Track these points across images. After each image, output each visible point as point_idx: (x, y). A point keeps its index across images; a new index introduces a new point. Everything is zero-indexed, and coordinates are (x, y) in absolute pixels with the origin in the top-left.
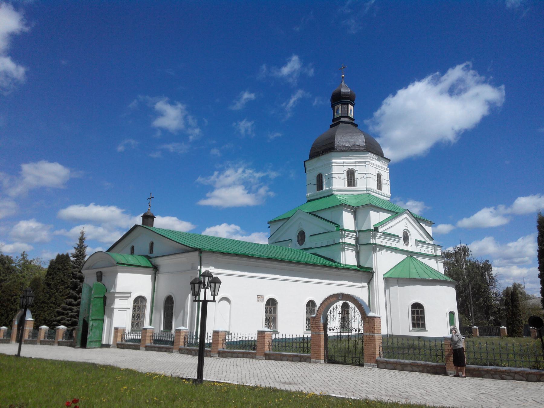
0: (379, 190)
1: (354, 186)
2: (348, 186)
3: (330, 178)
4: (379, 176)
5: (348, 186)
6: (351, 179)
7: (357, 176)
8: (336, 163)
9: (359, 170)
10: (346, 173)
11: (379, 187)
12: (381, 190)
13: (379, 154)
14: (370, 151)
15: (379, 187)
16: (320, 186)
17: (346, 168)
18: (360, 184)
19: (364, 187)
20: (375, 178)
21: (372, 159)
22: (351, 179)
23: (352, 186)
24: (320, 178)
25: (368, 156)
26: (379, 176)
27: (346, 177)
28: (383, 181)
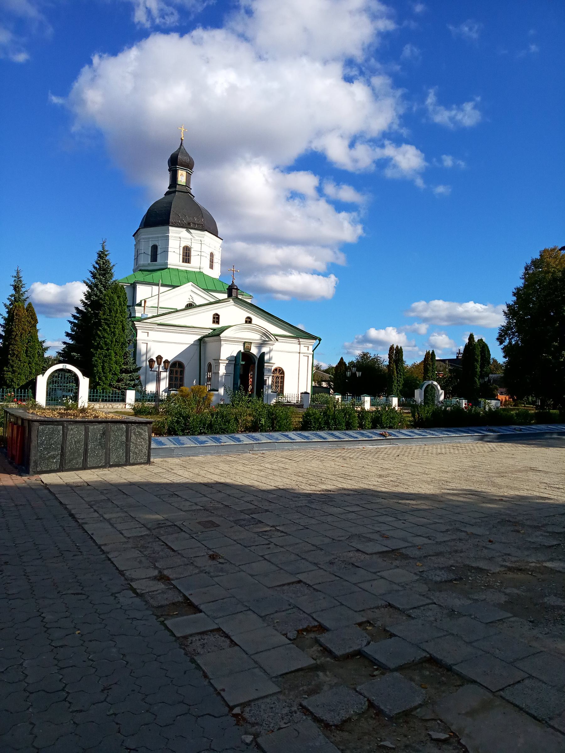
2: (183, 262)
3: (166, 251)
4: (212, 255)
5: (183, 262)
6: (187, 256)
7: (193, 253)
11: (211, 267)
12: (212, 269)
13: (215, 232)
14: (206, 230)
15: (211, 267)
16: (154, 258)
17: (183, 245)
20: (209, 257)
22: (187, 256)
23: (186, 262)
24: (155, 249)
25: (204, 235)
26: (212, 255)
27: (181, 253)
28: (215, 260)
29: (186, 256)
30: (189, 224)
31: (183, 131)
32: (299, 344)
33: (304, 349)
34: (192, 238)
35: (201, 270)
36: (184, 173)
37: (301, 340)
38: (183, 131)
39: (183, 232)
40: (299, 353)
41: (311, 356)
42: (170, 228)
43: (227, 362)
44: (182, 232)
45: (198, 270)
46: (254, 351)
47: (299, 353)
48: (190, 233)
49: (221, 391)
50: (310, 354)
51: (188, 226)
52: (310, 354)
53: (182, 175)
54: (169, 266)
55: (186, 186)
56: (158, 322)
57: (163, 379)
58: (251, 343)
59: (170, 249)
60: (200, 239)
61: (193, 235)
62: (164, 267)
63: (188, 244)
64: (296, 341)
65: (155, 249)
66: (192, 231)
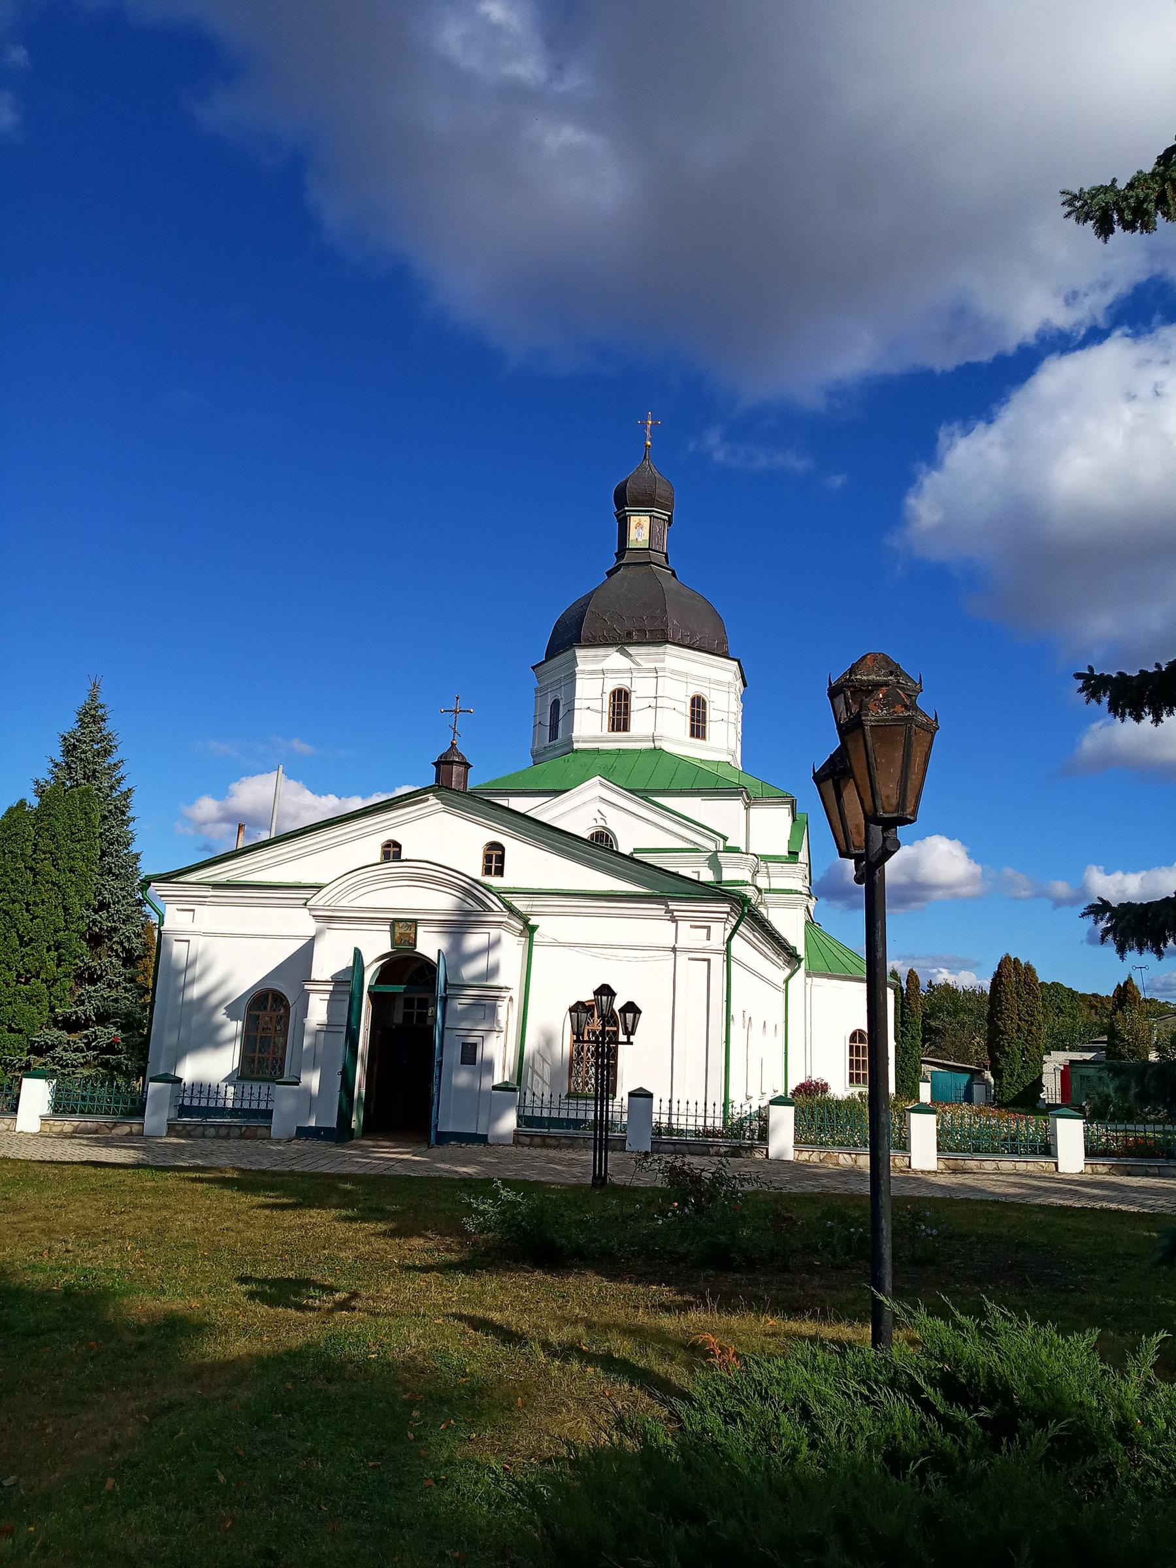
0: (698, 737)
1: (626, 729)
3: (571, 711)
4: (698, 706)
7: (635, 704)
8: (583, 672)
9: (641, 691)
10: (607, 698)
12: (704, 738)
14: (668, 642)
17: (611, 685)
18: (640, 722)
19: (648, 731)
21: (675, 658)
23: (619, 730)
24: (556, 704)
25: (664, 653)
26: (698, 706)
28: (711, 714)
29: (619, 714)
30: (629, 634)
31: (649, 426)
32: (674, 920)
33: (690, 936)
34: (633, 666)
35: (658, 744)
36: (645, 520)
37: (673, 906)
38: (649, 426)
39: (614, 659)
40: (674, 950)
41: (718, 961)
42: (580, 653)
43: (331, 988)
44: (608, 656)
45: (650, 745)
46: (429, 944)
47: (674, 950)
48: (628, 655)
49: (313, 1081)
50: (716, 952)
51: (622, 640)
52: (716, 952)
53: (639, 525)
54: (576, 746)
55: (649, 549)
56: (222, 879)
57: (232, 1040)
58: (415, 922)
59: (577, 704)
60: (652, 665)
61: (638, 659)
62: (568, 747)
63: (623, 682)
64: (657, 909)
65: (556, 704)
66: (632, 650)
